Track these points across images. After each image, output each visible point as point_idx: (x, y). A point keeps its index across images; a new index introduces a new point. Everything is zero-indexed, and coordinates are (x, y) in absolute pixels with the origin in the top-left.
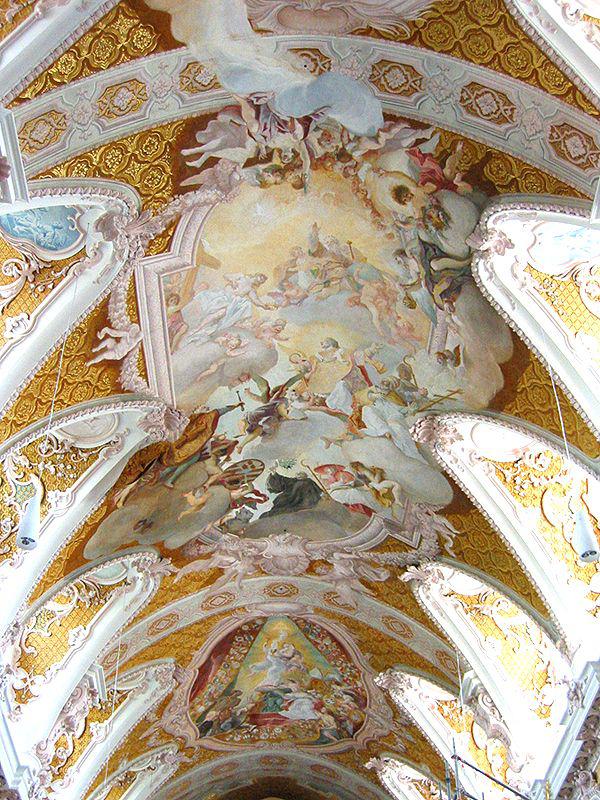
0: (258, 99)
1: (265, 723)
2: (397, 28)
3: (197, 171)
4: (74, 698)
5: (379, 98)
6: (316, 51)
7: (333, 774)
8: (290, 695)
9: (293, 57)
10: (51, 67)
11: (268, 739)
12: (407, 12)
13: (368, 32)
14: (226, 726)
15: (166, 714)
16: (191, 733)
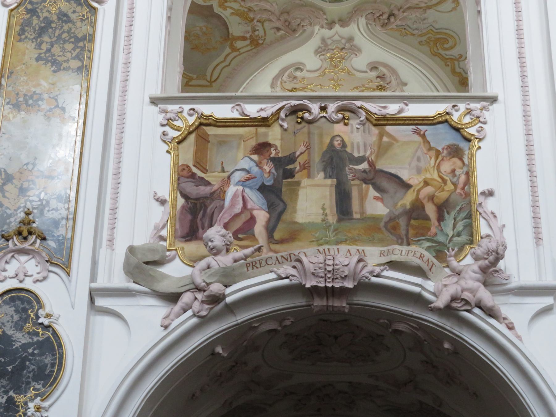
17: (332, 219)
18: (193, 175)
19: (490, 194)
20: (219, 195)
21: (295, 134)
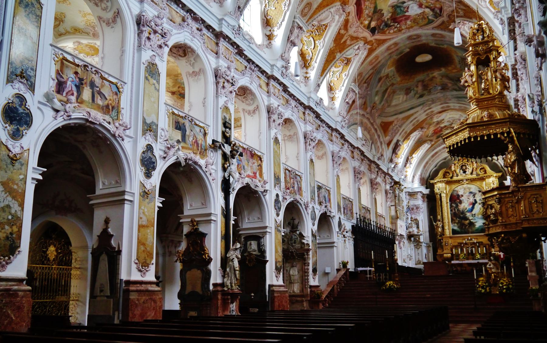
1: (401, 21)
4: (291, 32)
7: (442, 36)
8: (405, 5)
11: (407, 28)
14: (383, 28)
15: (349, 28)
16: (367, 34)
17: (91, 101)
18: (59, 74)
19: (123, 109)
20: (65, 83)
21: (84, 72)
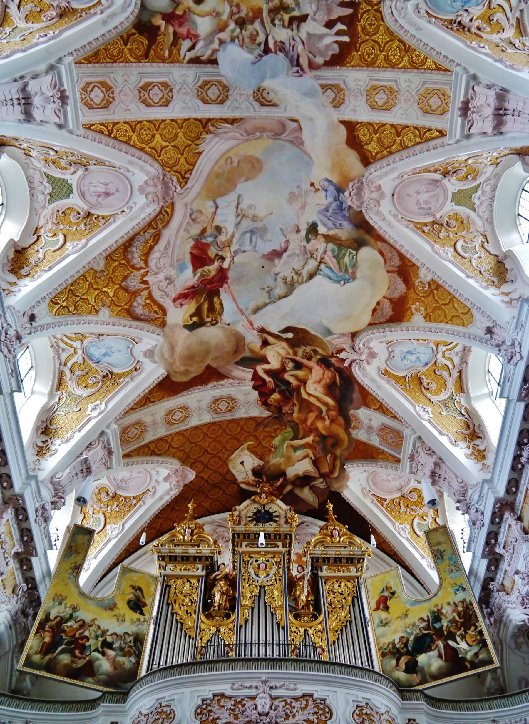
0: (297, 72)
2: (217, 128)
3: (340, 19)
5: (221, 76)
6: (263, 105)
9: (275, 101)
10: (419, 143)
12: (212, 139)
13: (233, 121)
